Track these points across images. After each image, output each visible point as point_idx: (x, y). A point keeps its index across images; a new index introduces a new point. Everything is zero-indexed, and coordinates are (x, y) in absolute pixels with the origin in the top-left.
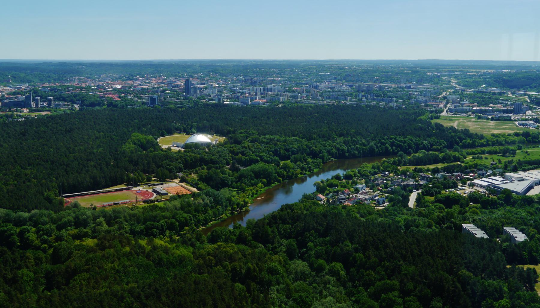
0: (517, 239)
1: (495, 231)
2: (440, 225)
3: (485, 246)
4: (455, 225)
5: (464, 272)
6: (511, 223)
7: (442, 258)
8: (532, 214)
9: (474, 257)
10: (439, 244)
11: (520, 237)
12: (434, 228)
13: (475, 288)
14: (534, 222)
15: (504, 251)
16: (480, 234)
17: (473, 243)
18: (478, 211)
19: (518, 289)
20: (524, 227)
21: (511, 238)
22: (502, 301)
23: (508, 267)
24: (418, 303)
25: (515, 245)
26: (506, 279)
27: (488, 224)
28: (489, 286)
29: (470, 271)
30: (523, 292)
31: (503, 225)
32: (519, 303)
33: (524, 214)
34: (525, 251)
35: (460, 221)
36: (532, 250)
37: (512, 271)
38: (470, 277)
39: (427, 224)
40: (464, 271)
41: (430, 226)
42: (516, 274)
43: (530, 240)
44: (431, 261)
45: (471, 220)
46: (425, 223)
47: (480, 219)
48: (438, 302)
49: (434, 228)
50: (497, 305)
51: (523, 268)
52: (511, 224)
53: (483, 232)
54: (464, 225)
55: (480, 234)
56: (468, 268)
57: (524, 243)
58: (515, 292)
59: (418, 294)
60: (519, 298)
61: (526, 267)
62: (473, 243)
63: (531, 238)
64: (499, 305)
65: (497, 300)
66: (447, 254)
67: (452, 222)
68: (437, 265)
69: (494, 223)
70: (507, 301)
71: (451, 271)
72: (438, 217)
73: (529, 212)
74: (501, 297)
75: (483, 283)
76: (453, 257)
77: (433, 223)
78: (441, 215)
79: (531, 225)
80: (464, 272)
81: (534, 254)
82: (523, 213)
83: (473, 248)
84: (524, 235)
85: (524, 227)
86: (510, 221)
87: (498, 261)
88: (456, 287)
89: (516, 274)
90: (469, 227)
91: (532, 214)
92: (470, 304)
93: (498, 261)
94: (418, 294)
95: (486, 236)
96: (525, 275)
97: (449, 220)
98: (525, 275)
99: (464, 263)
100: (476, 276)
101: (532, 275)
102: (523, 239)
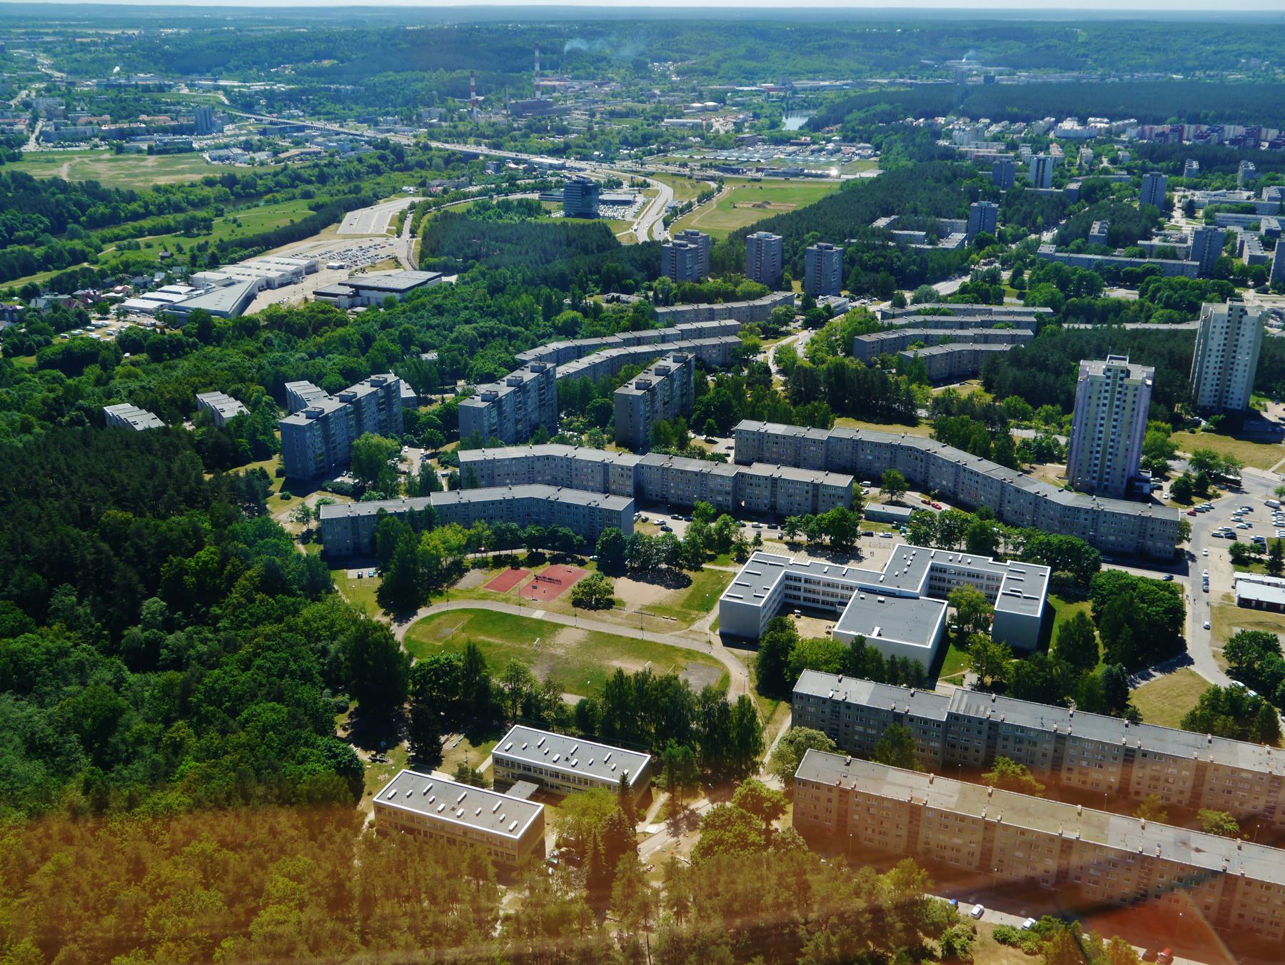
0: (225, 415)
1: (177, 406)
2: (52, 420)
3: (156, 446)
4: (88, 412)
5: (115, 514)
6: (211, 384)
7: (57, 496)
8: (252, 355)
9: (130, 477)
10: (49, 467)
11: (229, 407)
12: (37, 430)
13: (140, 543)
14: (258, 370)
15: (198, 447)
16: (144, 420)
17: (128, 446)
18: (138, 371)
19: (230, 519)
20: (239, 386)
21: (212, 416)
22: (201, 553)
23: (207, 477)
24: (19, 611)
25: (221, 429)
26: (207, 507)
27: (162, 395)
28: (171, 530)
29: (125, 509)
30: (246, 522)
31: (195, 392)
32: (236, 547)
33: (237, 359)
34: (242, 437)
35: (100, 400)
36: (256, 430)
37: (216, 485)
38: (128, 522)
39: (18, 425)
40: (112, 512)
41: (26, 428)
42: (224, 488)
43: (253, 411)
44: (35, 510)
45: (124, 393)
46: (11, 424)
47: (142, 387)
48: (66, 595)
49: (37, 430)
50: (193, 564)
51: (237, 475)
52: (210, 385)
53: (153, 415)
54: (109, 410)
55: (144, 420)
56: (121, 504)
57: (239, 420)
58: (225, 527)
59: (15, 591)
60: (235, 537)
61: (242, 471)
62: (128, 446)
63: (254, 406)
64: (197, 563)
65: (190, 554)
66: (69, 484)
67: (80, 408)
68: (49, 515)
69: (176, 391)
70: (212, 549)
71: (86, 520)
72: (44, 402)
73: (247, 352)
74: (200, 547)
75: (157, 527)
76: (85, 488)
77: (32, 419)
78: (52, 395)
79: (252, 380)
80: (115, 514)
81: (261, 438)
82: (235, 356)
83: (129, 456)
84: (239, 403)
85: (239, 386)
86: (208, 380)
87: (183, 471)
88: (99, 551)
89: (224, 488)
90: (121, 410)
91: (252, 355)
92: (135, 578)
93: (183, 471)
94: (15, 591)
95: (158, 423)
96: (243, 486)
97: (72, 405)
98: (243, 486)
99: (112, 494)
100: (142, 515)
101: (256, 483)
102: (234, 414)
